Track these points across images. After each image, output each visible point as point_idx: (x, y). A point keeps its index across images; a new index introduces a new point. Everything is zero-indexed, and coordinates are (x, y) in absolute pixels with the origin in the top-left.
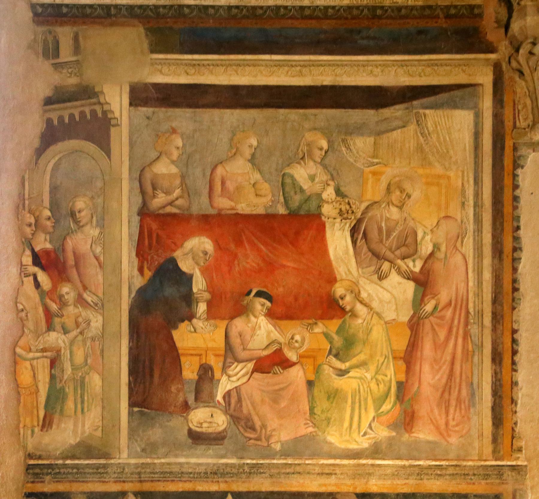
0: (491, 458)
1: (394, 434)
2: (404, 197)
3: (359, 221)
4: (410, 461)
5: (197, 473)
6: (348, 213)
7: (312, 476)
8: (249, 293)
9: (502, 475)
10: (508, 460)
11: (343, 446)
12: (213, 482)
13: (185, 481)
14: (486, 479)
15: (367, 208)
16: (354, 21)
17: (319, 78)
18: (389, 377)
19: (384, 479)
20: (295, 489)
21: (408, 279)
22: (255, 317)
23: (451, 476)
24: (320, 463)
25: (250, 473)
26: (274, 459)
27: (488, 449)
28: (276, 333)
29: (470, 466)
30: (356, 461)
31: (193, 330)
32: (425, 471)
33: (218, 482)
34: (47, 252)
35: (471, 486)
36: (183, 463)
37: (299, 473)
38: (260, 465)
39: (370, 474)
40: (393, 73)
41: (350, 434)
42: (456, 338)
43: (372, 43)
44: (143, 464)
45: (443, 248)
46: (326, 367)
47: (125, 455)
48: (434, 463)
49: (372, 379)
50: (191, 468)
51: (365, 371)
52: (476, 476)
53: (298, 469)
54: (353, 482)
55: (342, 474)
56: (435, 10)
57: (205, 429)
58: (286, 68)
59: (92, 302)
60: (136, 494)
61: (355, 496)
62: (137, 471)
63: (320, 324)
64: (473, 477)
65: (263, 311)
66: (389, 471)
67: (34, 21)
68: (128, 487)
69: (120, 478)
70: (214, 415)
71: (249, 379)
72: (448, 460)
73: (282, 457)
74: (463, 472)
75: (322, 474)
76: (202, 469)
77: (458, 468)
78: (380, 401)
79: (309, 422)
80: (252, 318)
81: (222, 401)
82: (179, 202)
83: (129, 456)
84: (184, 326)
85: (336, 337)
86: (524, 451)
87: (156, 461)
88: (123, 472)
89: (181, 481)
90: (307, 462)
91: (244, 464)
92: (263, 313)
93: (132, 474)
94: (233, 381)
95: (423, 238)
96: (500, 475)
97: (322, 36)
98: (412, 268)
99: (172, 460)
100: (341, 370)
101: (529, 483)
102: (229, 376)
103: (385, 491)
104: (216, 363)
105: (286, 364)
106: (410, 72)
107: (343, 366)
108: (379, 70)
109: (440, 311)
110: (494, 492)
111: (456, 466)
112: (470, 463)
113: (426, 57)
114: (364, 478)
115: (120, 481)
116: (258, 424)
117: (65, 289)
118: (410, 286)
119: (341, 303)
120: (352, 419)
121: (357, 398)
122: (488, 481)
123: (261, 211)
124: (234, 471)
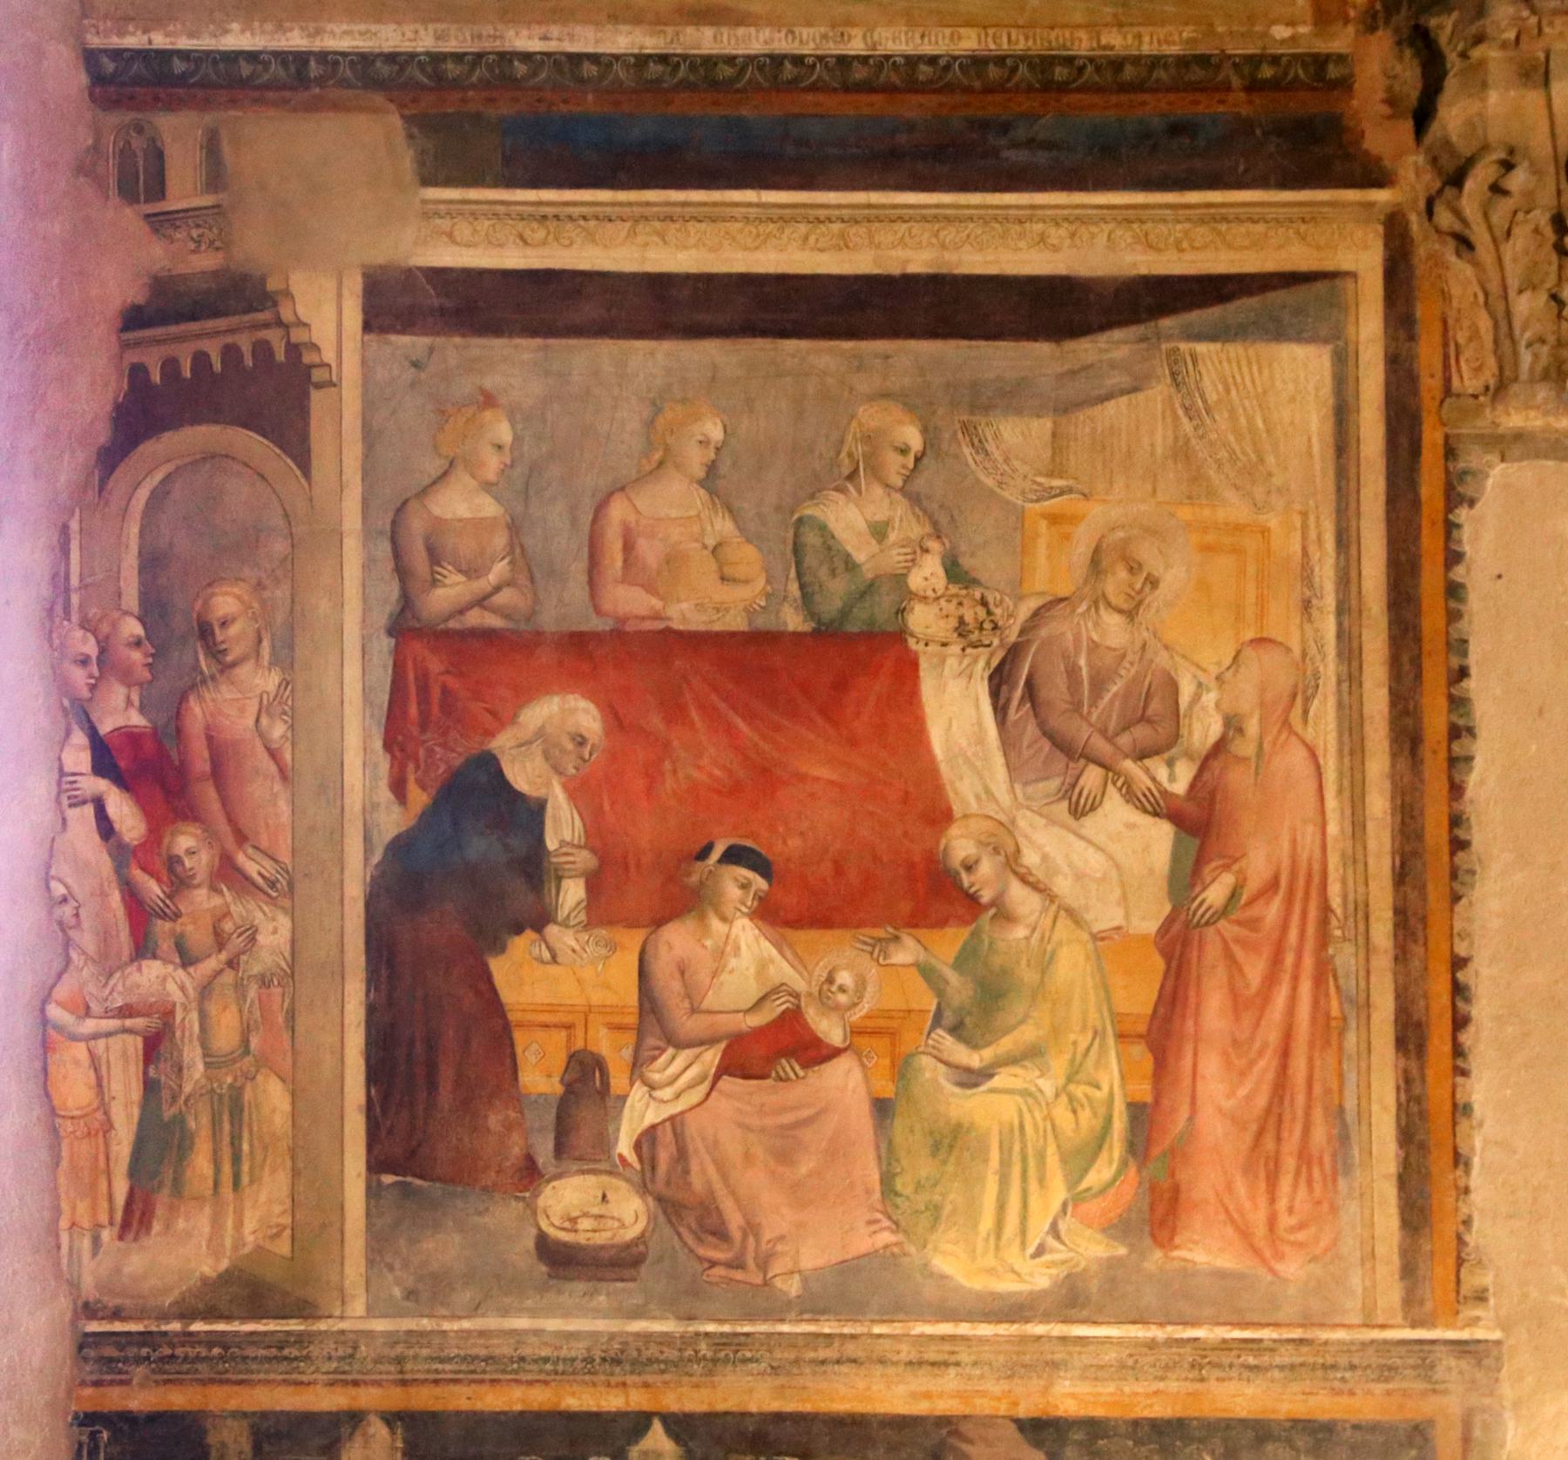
0: (1399, 1320)
1: (1122, 1251)
2: (1138, 586)
3: (1014, 653)
4: (1169, 1328)
5: (564, 1360)
6: (981, 628)
7: (891, 1370)
8: (704, 853)
9: (1432, 1367)
10: (1448, 1326)
11: (978, 1284)
12: (609, 1385)
13: (530, 1383)
14: (1387, 1380)
15: (1036, 614)
16: (990, 98)
17: (893, 253)
18: (1106, 1088)
19: (1096, 1379)
20: (841, 1406)
21: (1156, 814)
22: (724, 919)
23: (1287, 1373)
24: (913, 1333)
25: (715, 1361)
26: (782, 1320)
27: (1391, 1294)
28: (785, 964)
29: (1340, 1342)
30: (1014, 1329)
31: (546, 955)
32: (1213, 1357)
33: (624, 1384)
34: (131, 737)
35: (1345, 1400)
36: (526, 1332)
37: (854, 1361)
38: (743, 1339)
39: (1055, 1365)
40: (1102, 239)
41: (997, 1248)
42: (1295, 979)
43: (1042, 157)
44: (409, 1333)
45: (1252, 727)
46: (926, 1061)
47: (358, 1307)
48: (1237, 1334)
49: (1057, 1095)
50: (546, 1344)
51: (1037, 1073)
52: (1359, 1372)
53: (851, 1349)
54: (1006, 1388)
55: (975, 1364)
56: (1218, 67)
57: (586, 1234)
58: (803, 228)
59: (260, 874)
60: (392, 1419)
61: (1013, 1426)
62: (393, 1354)
63: (908, 941)
64: (1348, 1375)
65: (744, 904)
66: (1110, 1356)
67: (91, 95)
68: (367, 1398)
69: (344, 1373)
70: (609, 1196)
71: (708, 1095)
72: (1276, 1325)
73: (806, 1316)
74: (1321, 1361)
75: (921, 1363)
76: (578, 1349)
77: (1305, 1349)
78: (1081, 1157)
79: (879, 1216)
80: (716, 924)
81: (631, 1157)
82: (503, 598)
83: (371, 1312)
84: (522, 945)
85: (953, 977)
86: (1492, 1301)
87: (446, 1326)
88: (352, 1356)
89: (517, 1381)
90: (877, 1330)
91: (697, 1334)
92: (745, 910)
93: (378, 1361)
94: (662, 1101)
95: (1196, 698)
96: (1425, 1368)
97: (902, 139)
98: (1166, 784)
99: (492, 1322)
100: (968, 1070)
101: (1507, 1390)
102: (652, 1087)
103: (1099, 1412)
104: (613, 1049)
105: (814, 1053)
106: (1151, 237)
107: (974, 1060)
108: (1062, 232)
109: (1250, 903)
110: (1409, 1416)
111: (1302, 1341)
112: (1340, 1335)
113: (1194, 197)
114: (1039, 1377)
115: (345, 1383)
116: (735, 1221)
117: (185, 841)
118: (1162, 835)
119: (966, 879)
120: (1001, 1207)
121: (1017, 1148)
122: (1390, 1386)
123: (735, 622)
124: (672, 1354)
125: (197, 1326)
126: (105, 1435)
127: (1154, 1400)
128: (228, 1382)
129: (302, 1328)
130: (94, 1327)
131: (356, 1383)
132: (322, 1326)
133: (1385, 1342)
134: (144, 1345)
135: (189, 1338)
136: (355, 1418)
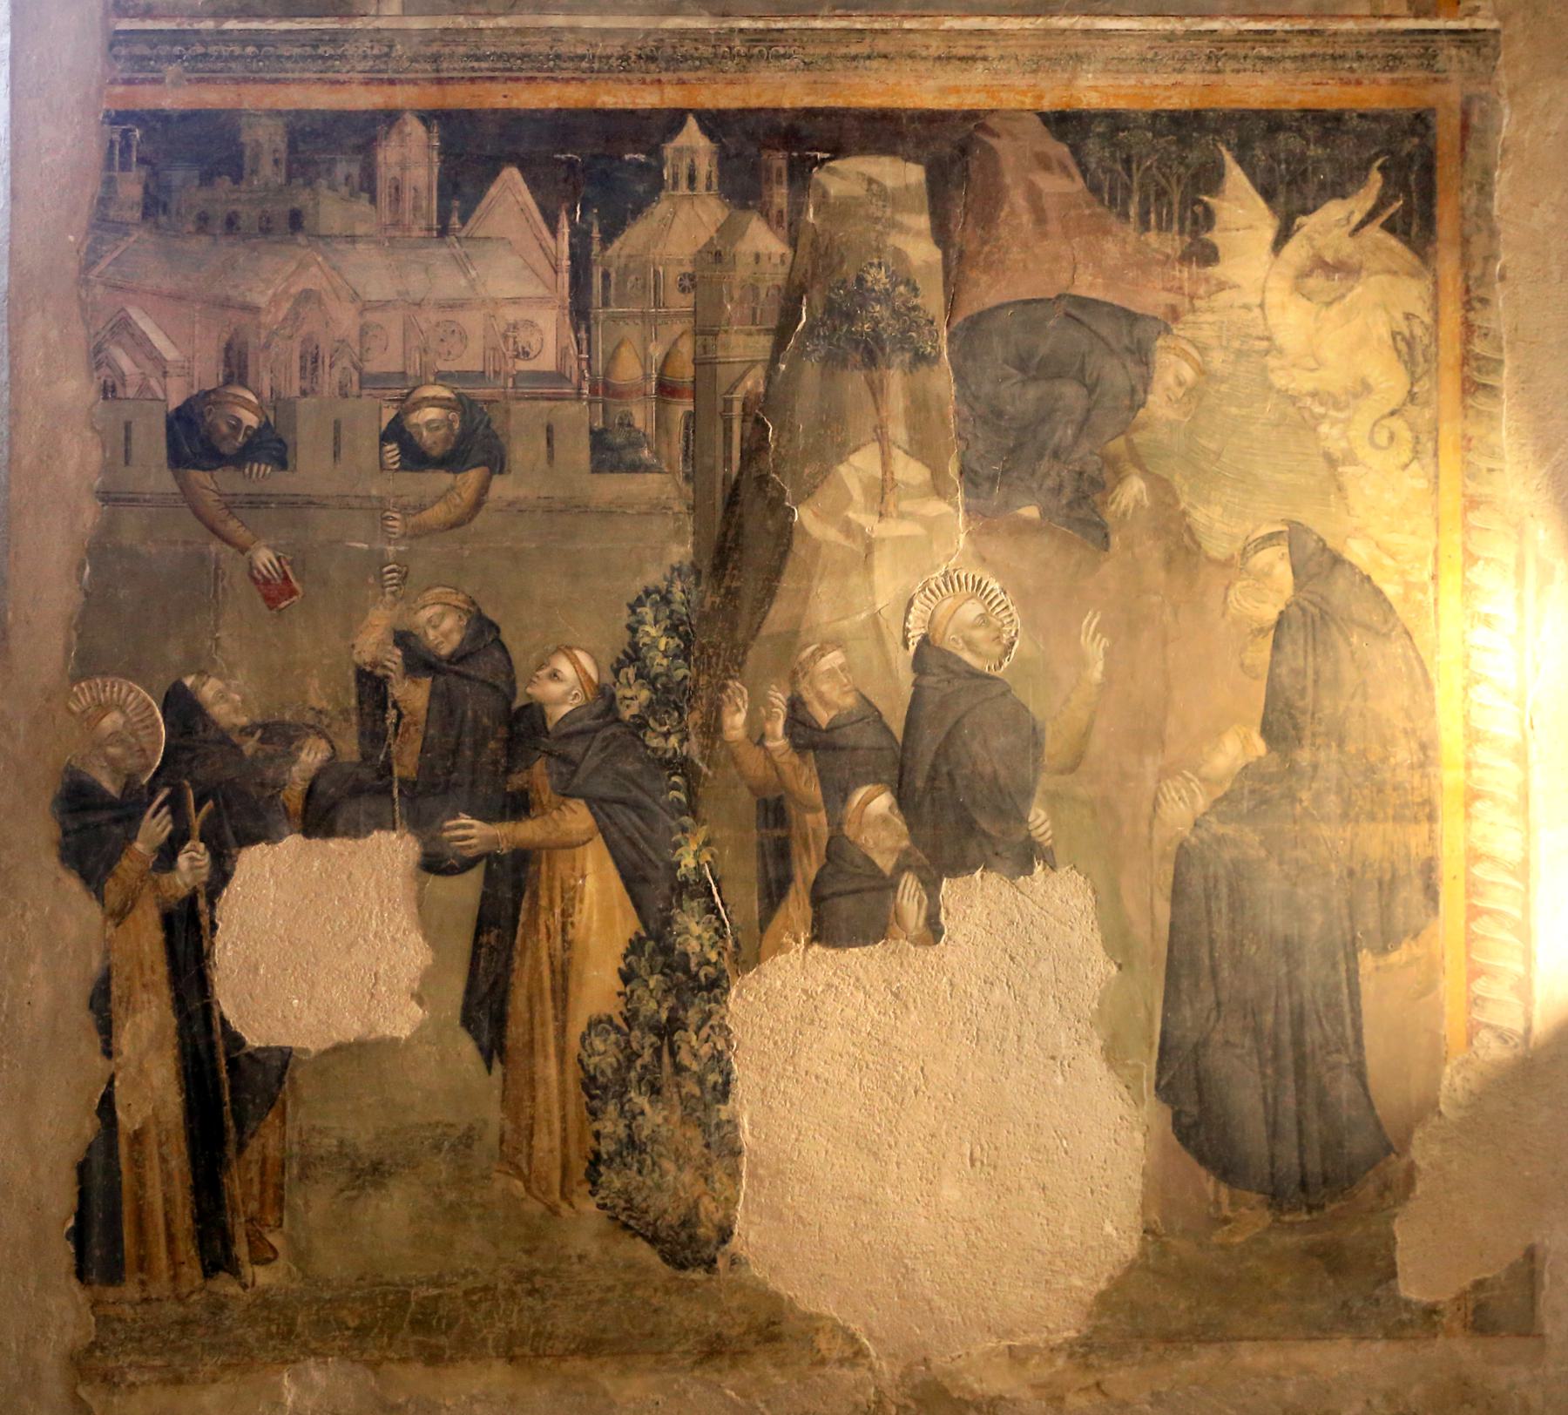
0: (1404, 10)
4: (1188, 21)
5: (600, 58)
7: (921, 67)
9: (1435, 56)
10: (1450, 16)
12: (644, 82)
13: (567, 81)
14: (1392, 70)
19: (1118, 71)
20: (872, 102)
23: (1299, 64)
25: (749, 57)
29: (1349, 33)
32: (1229, 49)
33: (659, 81)
35: (1351, 90)
36: (562, 29)
38: (776, 35)
39: (1078, 58)
48: (1252, 25)
50: (583, 42)
52: (1365, 62)
53: (882, 45)
54: (1033, 81)
55: (1002, 58)
60: (426, 117)
61: (1037, 119)
62: (430, 51)
64: (1355, 65)
66: (1131, 49)
68: (402, 96)
69: (379, 71)
72: (1290, 17)
73: (838, 12)
74: (1331, 51)
75: (949, 58)
76: (614, 47)
77: (1315, 40)
83: (406, 10)
87: (482, 24)
88: (387, 55)
89: (555, 80)
90: (907, 25)
91: (732, 30)
93: (413, 60)
96: (1428, 58)
99: (528, 20)
101: (1503, 78)
103: (1121, 105)
110: (1412, 105)
111: (1312, 32)
112: (1349, 25)
114: (1064, 70)
115: (381, 81)
122: (1395, 75)
124: (706, 51)
125: (231, 25)
126: (137, 133)
127: (1173, 92)
128: (263, 80)
129: (337, 26)
130: (125, 25)
131: (392, 82)
132: (358, 24)
133: (1392, 32)
134: (174, 43)
135: (222, 36)
136: (391, 117)
